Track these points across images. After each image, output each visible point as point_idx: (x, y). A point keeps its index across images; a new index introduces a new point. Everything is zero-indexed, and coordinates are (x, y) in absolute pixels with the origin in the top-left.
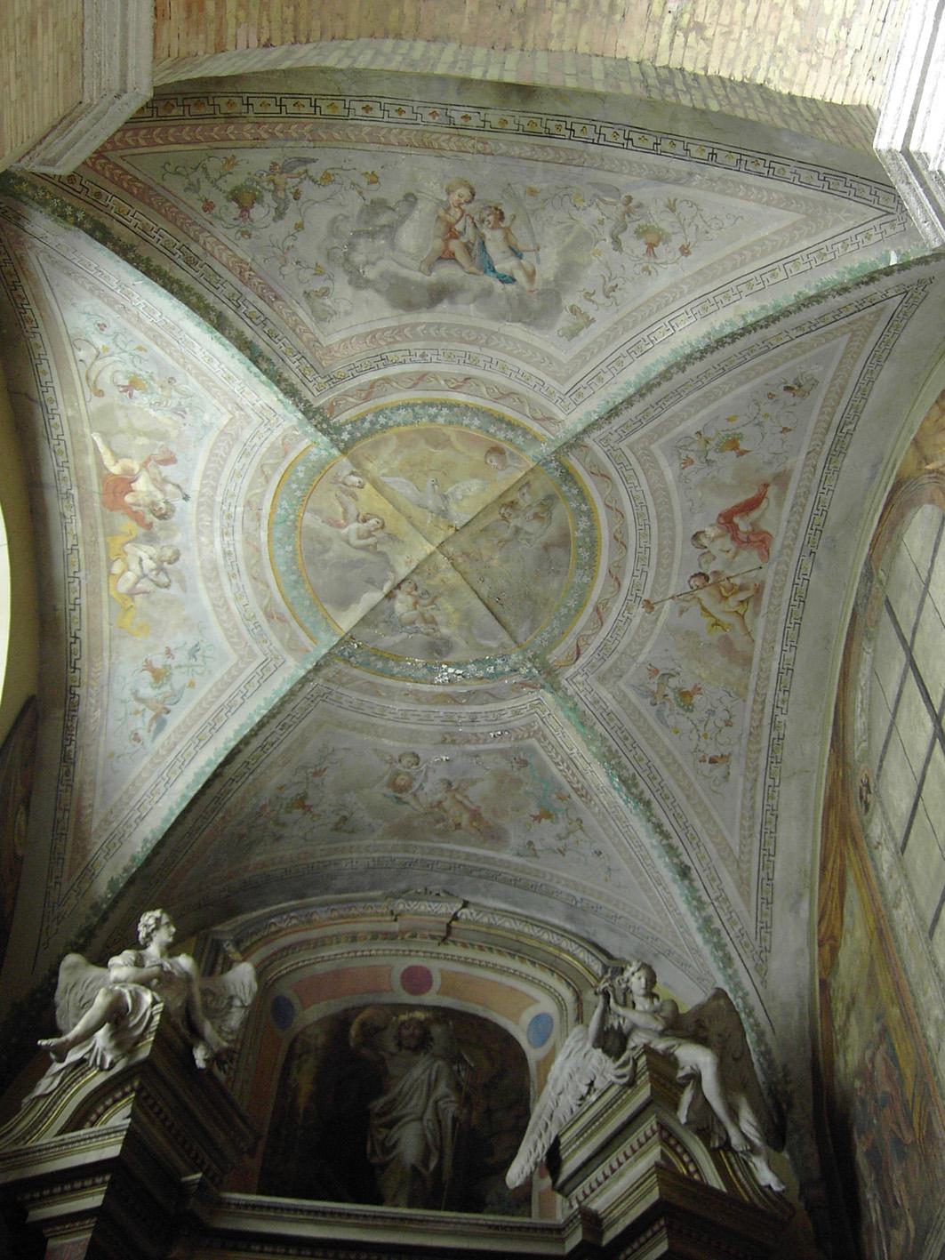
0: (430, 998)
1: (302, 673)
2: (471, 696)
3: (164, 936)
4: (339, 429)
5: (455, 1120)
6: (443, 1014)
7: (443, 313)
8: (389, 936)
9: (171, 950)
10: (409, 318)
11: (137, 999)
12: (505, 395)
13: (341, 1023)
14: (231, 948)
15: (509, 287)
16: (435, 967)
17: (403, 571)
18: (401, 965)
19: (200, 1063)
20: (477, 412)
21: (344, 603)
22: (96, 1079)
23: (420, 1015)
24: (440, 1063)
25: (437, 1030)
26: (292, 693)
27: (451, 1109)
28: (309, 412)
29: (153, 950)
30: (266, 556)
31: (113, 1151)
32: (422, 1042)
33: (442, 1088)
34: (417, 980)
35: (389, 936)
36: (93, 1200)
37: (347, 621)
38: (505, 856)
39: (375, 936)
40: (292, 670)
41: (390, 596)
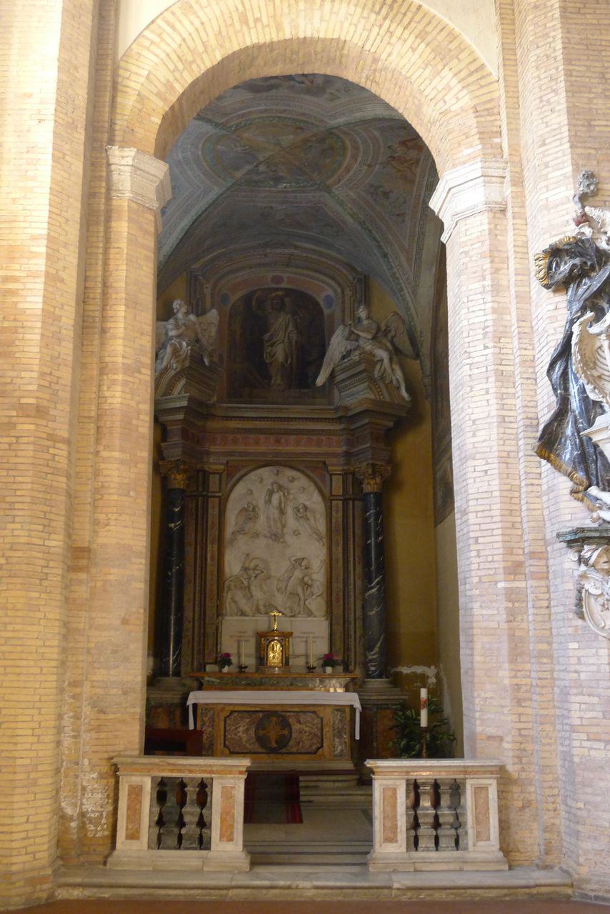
0: (284, 285)
1: (221, 192)
2: (293, 192)
3: (184, 310)
4: (231, 127)
5: (296, 342)
6: (289, 292)
7: (274, 92)
8: (264, 265)
9: (187, 313)
10: (260, 95)
11: (181, 345)
12: (304, 114)
13: (247, 299)
14: (201, 278)
15: (302, 85)
16: (285, 276)
17: (261, 159)
18: (271, 275)
19: (207, 364)
20: (290, 119)
21: (237, 168)
22: (172, 373)
23: (280, 293)
24: (289, 316)
25: (287, 300)
26: (217, 199)
27: (294, 337)
28: (217, 125)
29: (180, 315)
30: (202, 157)
31: (185, 403)
32: (280, 307)
33: (291, 328)
34: (278, 280)
35: (264, 265)
36: (180, 416)
37: (239, 174)
38: (311, 234)
39: (259, 265)
40: (215, 192)
41: (256, 166)
